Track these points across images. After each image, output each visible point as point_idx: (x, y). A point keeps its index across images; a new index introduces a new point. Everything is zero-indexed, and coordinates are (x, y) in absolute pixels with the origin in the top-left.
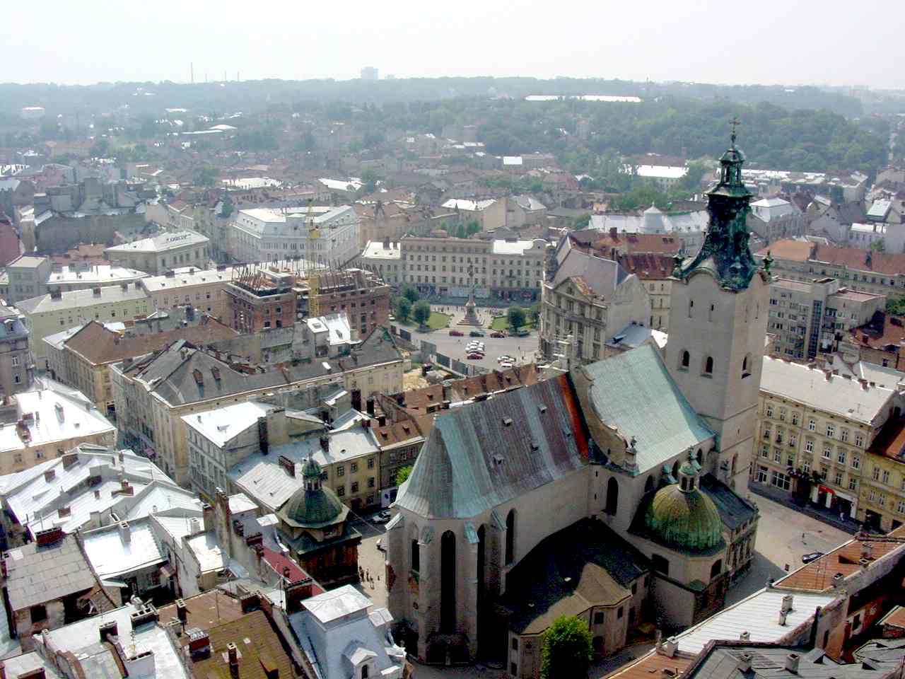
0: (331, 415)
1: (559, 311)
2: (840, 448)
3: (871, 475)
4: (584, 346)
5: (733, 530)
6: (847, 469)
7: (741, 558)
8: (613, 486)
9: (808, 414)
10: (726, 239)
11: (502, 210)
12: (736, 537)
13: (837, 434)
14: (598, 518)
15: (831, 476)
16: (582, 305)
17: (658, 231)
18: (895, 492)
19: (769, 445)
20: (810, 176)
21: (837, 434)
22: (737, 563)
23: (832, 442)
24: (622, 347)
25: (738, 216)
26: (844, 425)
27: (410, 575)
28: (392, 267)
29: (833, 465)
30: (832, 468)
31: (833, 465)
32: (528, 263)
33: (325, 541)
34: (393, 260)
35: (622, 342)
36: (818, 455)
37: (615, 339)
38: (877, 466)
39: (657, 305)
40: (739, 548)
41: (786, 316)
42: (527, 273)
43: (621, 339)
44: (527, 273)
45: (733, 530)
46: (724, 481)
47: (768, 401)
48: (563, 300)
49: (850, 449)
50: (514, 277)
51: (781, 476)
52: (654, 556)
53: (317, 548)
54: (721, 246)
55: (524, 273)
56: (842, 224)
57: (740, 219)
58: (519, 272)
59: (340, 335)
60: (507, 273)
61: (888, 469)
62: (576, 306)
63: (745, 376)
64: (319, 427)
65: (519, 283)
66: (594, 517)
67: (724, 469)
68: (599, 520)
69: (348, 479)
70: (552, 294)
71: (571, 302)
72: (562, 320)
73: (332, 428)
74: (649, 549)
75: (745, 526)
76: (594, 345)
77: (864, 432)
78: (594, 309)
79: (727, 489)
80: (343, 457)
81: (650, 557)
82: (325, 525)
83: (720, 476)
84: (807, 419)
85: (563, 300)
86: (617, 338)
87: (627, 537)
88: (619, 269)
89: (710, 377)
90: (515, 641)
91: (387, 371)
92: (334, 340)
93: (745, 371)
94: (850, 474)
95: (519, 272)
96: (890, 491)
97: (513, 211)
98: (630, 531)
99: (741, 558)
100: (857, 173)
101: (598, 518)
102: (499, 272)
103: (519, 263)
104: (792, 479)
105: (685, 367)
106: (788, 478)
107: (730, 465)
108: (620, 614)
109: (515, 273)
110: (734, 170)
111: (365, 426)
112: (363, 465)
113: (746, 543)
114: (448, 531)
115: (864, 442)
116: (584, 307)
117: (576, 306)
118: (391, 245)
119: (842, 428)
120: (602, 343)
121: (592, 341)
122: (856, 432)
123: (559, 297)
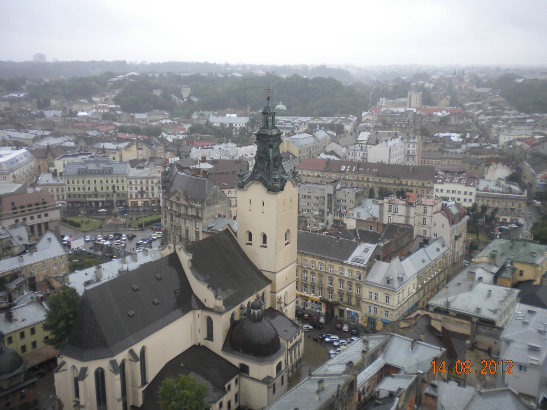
0: (13, 296)
1: (172, 212)
2: (348, 282)
3: (368, 297)
4: (189, 232)
5: (288, 341)
6: (354, 295)
7: (295, 357)
8: (210, 323)
9: (329, 263)
10: (269, 161)
11: (134, 148)
12: (290, 345)
13: (346, 274)
15: (345, 299)
16: (187, 208)
17: (233, 157)
18: (382, 305)
19: (307, 284)
20: (325, 118)
21: (346, 274)
22: (293, 362)
23: (344, 279)
24: (213, 232)
25: (274, 146)
26: (350, 268)
27: (75, 403)
28: (60, 190)
29: (345, 293)
30: (345, 294)
31: (345, 293)
32: (152, 182)
33: (10, 388)
34: (60, 185)
35: (213, 228)
36: (336, 286)
37: (208, 227)
38: (371, 291)
39: (233, 204)
40: (294, 351)
41: (312, 205)
42: (153, 189)
43: (212, 227)
44: (153, 189)
45: (288, 341)
47: (304, 258)
48: (174, 205)
49: (354, 282)
50: (144, 192)
51: (316, 302)
52: (241, 365)
53: (5, 393)
54: (266, 166)
55: (150, 188)
56: (342, 147)
57: (275, 149)
58: (147, 189)
59: (21, 239)
60: (139, 189)
61: (377, 292)
62: (182, 208)
63: (286, 244)
64: (4, 305)
65: (147, 195)
66: (199, 344)
67: (280, 303)
68: (203, 346)
69: (29, 339)
70: (167, 201)
71: (179, 206)
72: (174, 218)
73: (15, 305)
74: (236, 361)
75: (295, 337)
76: (196, 231)
77: (362, 271)
78: (194, 210)
79: (283, 315)
80: (24, 324)
81: (237, 365)
82: (10, 375)
83: (277, 308)
84: (327, 267)
85: (174, 205)
86: (209, 226)
87: (221, 354)
88: (208, 183)
89: (266, 247)
91: (56, 261)
92: (16, 242)
93: (286, 242)
94: (356, 297)
95: (147, 189)
96: (379, 304)
97: (141, 149)
99: (295, 357)
100: (351, 115)
101: (201, 345)
102: (134, 188)
103: (147, 182)
104: (323, 304)
106: (320, 304)
107: (283, 300)
108: (221, 405)
109: (144, 189)
110: (270, 118)
111: (40, 301)
112: (39, 330)
113: (297, 348)
114: (99, 368)
115: (362, 276)
116: (187, 208)
117: (182, 208)
118: (58, 175)
119: (348, 270)
120: (200, 230)
121: (194, 229)
122: (357, 272)
123: (171, 203)
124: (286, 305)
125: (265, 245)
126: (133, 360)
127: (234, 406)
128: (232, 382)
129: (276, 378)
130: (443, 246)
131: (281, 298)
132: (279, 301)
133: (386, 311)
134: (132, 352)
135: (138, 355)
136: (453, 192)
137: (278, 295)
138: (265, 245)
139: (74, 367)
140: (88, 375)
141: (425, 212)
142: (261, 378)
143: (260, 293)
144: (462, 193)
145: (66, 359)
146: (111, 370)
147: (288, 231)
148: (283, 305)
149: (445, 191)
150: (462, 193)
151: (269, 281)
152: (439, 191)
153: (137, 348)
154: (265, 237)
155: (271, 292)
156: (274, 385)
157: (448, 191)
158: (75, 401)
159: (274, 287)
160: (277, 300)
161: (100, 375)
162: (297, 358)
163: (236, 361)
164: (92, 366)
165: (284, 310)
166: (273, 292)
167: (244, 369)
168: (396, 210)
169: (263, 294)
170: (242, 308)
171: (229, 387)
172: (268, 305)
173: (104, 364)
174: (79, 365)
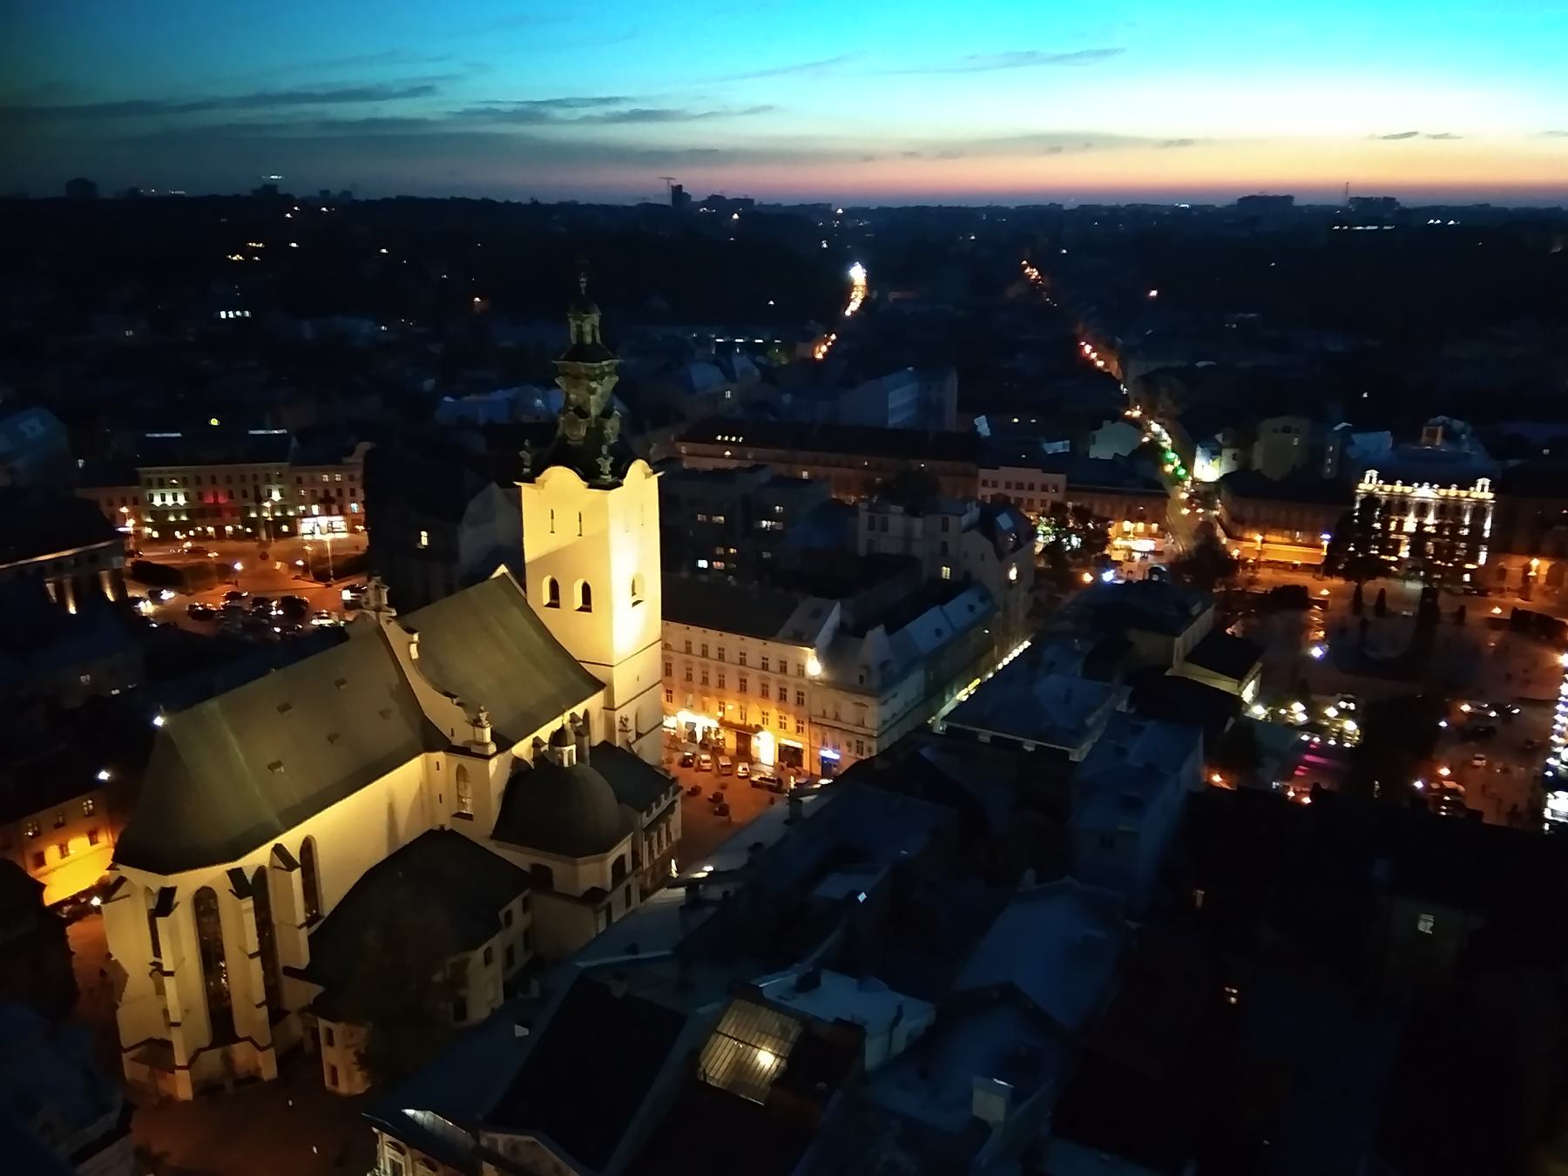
7: (660, 845)
14: (447, 828)
22: (656, 853)
40: (655, 834)
46: (625, 747)
52: (535, 866)
66: (442, 827)
67: (624, 730)
68: (451, 831)
81: (525, 867)
90: (330, 1032)
93: (635, 599)
98: (499, 833)
99: (660, 845)
100: (812, 321)
101: (447, 828)
105: (554, 602)
107: (631, 725)
109: (333, 494)
113: (663, 826)
124: (639, 736)
125: (587, 606)
126: (284, 867)
127: (521, 959)
128: (516, 905)
129: (612, 890)
130: (982, 600)
131: (626, 719)
132: (624, 728)
133: (858, 742)
134: (279, 850)
135: (295, 855)
136: (1020, 486)
137: (617, 715)
138: (587, 606)
139: (148, 889)
140: (178, 903)
141: (945, 528)
142: (580, 893)
143: (579, 710)
144: (1038, 487)
145: (125, 871)
146: (231, 891)
147: (639, 575)
148: (632, 736)
149: (1002, 485)
150: (1038, 487)
151: (597, 685)
152: (990, 484)
153: (291, 840)
154: (586, 589)
155: (604, 708)
156: (609, 905)
157: (1008, 486)
158: (153, 964)
159: (610, 697)
160: (618, 725)
161: (205, 901)
162: (665, 848)
163: (520, 858)
164: (187, 882)
165: (635, 748)
166: (610, 707)
167: (540, 879)
168: (885, 528)
169: (586, 713)
170: (537, 744)
171: (509, 915)
172: (598, 736)
173: (214, 875)
174: (157, 882)
